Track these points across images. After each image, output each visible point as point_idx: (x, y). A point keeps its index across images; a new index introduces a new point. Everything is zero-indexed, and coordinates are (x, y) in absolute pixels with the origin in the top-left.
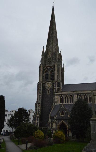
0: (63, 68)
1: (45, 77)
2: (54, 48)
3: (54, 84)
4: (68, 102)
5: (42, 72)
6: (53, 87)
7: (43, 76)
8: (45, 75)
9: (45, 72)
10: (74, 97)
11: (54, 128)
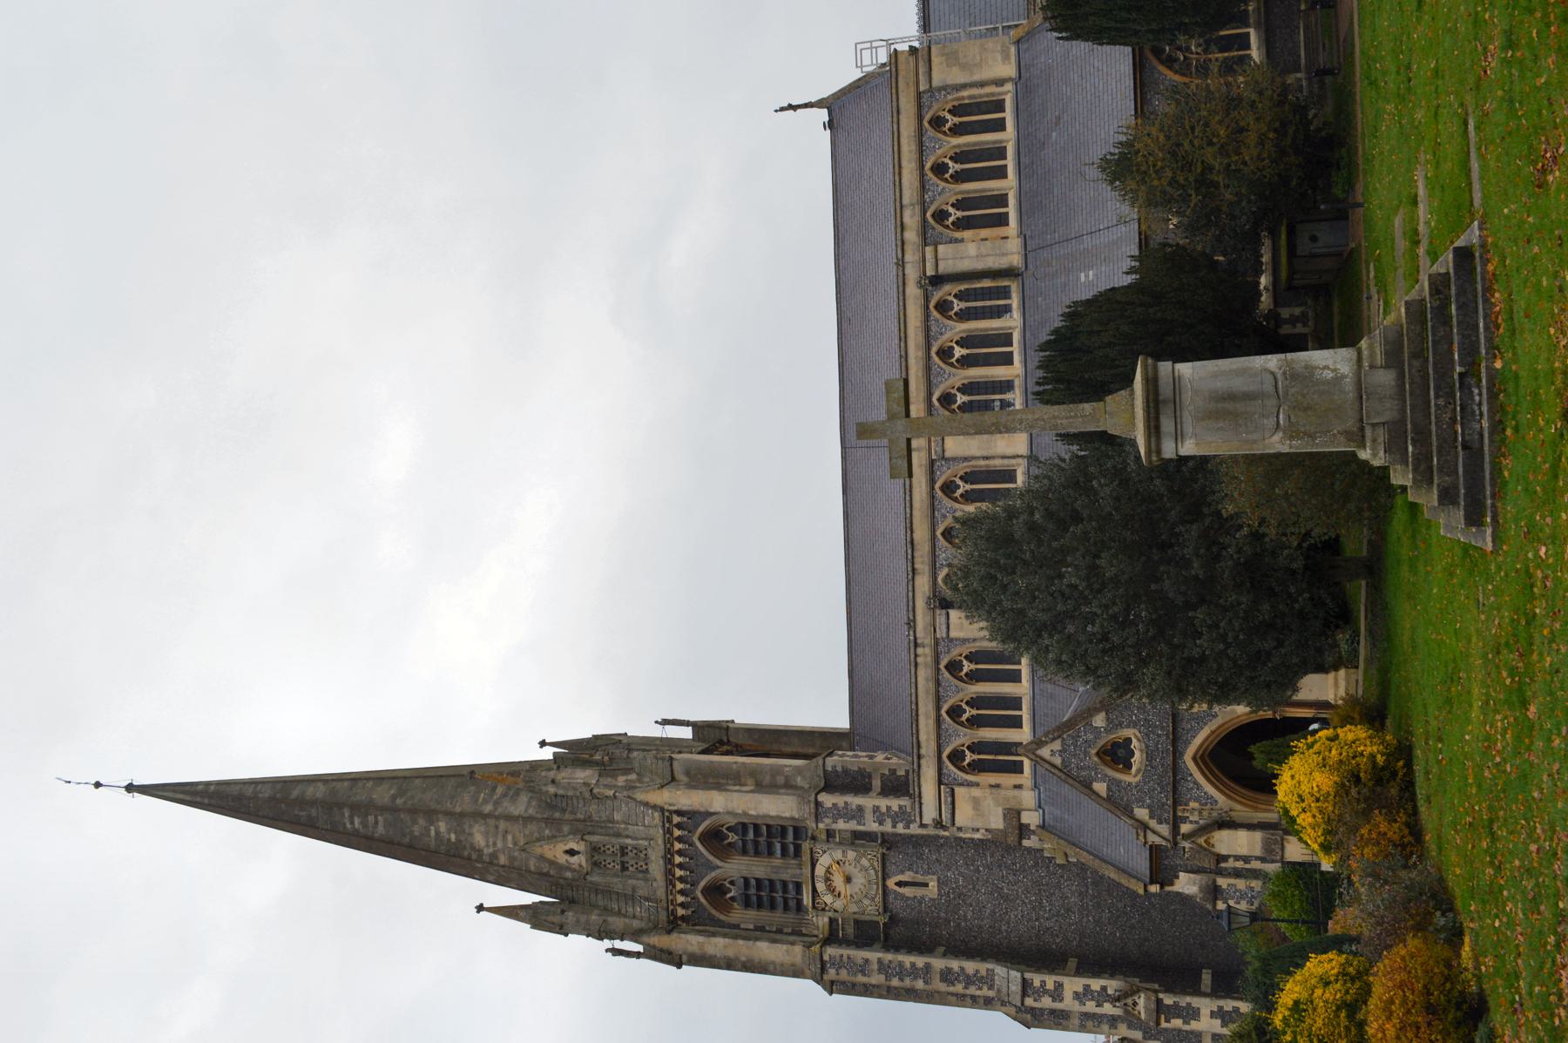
0: (698, 727)
1: (764, 916)
2: (496, 803)
3: (841, 825)
4: (1015, 703)
5: (717, 945)
6: (868, 837)
7: (761, 929)
8: (752, 914)
9: (725, 907)
10: (964, 641)
11: (1258, 852)
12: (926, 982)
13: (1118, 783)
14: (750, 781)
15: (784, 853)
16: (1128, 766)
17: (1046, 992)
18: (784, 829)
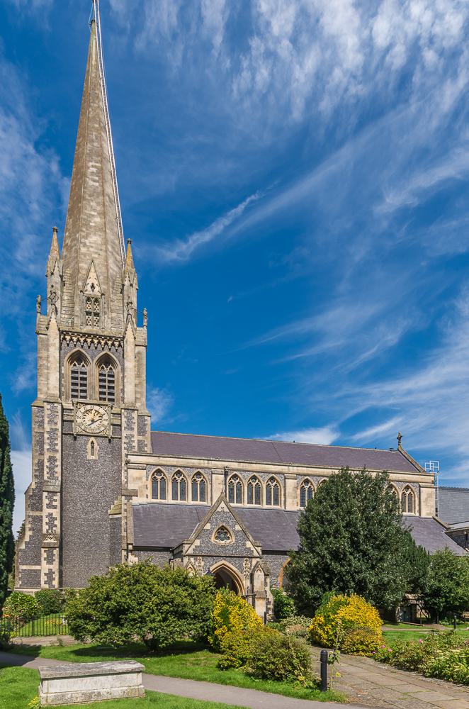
12: (48, 449)
14: (137, 382)
16: (216, 538)
17: (51, 501)
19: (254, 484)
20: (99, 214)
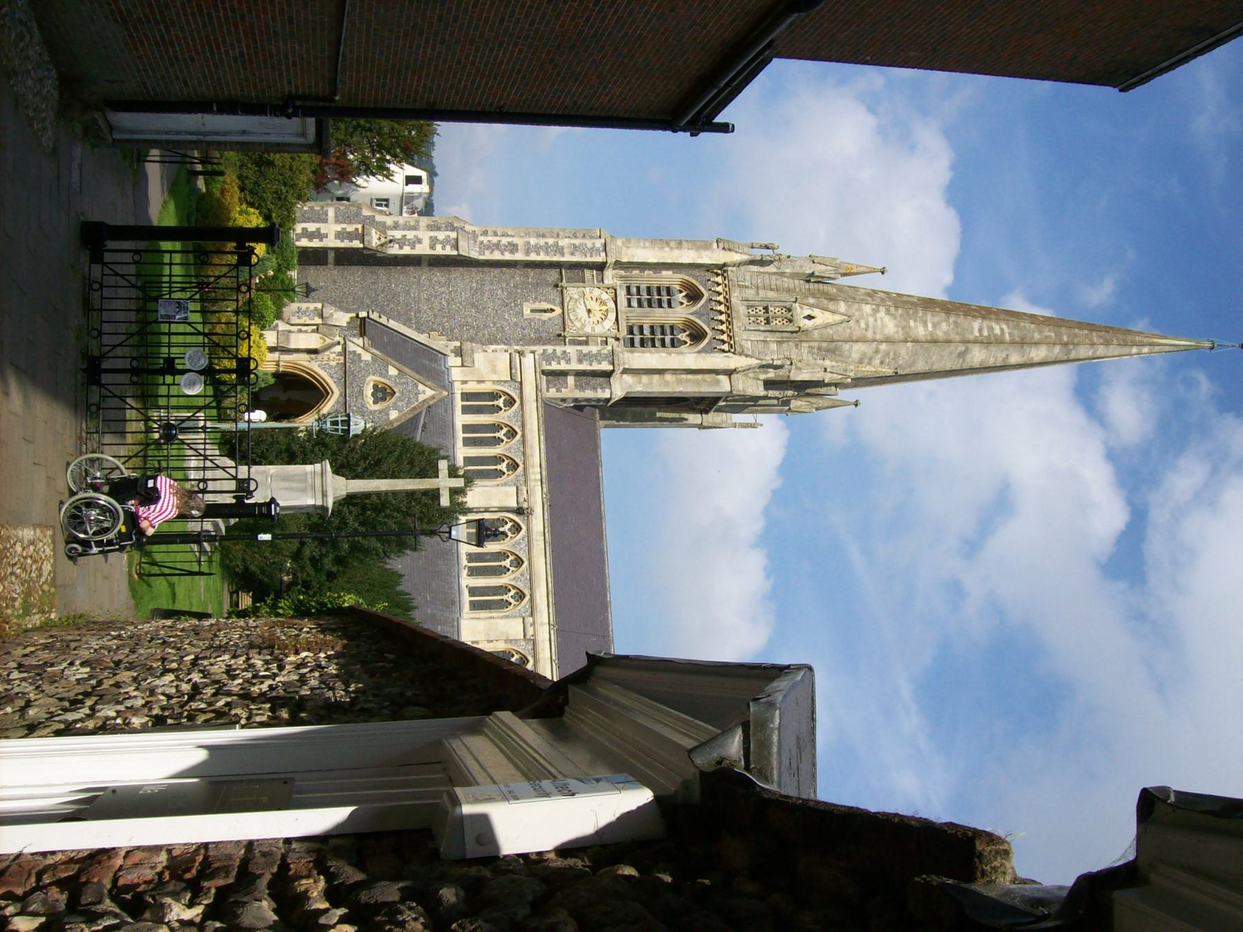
2: (877, 351)
6: (575, 342)
8: (665, 283)
10: (505, 484)
11: (293, 336)
13: (381, 375)
15: (641, 328)
16: (375, 387)
17: (442, 242)
18: (642, 344)
19: (507, 563)
20: (931, 334)
